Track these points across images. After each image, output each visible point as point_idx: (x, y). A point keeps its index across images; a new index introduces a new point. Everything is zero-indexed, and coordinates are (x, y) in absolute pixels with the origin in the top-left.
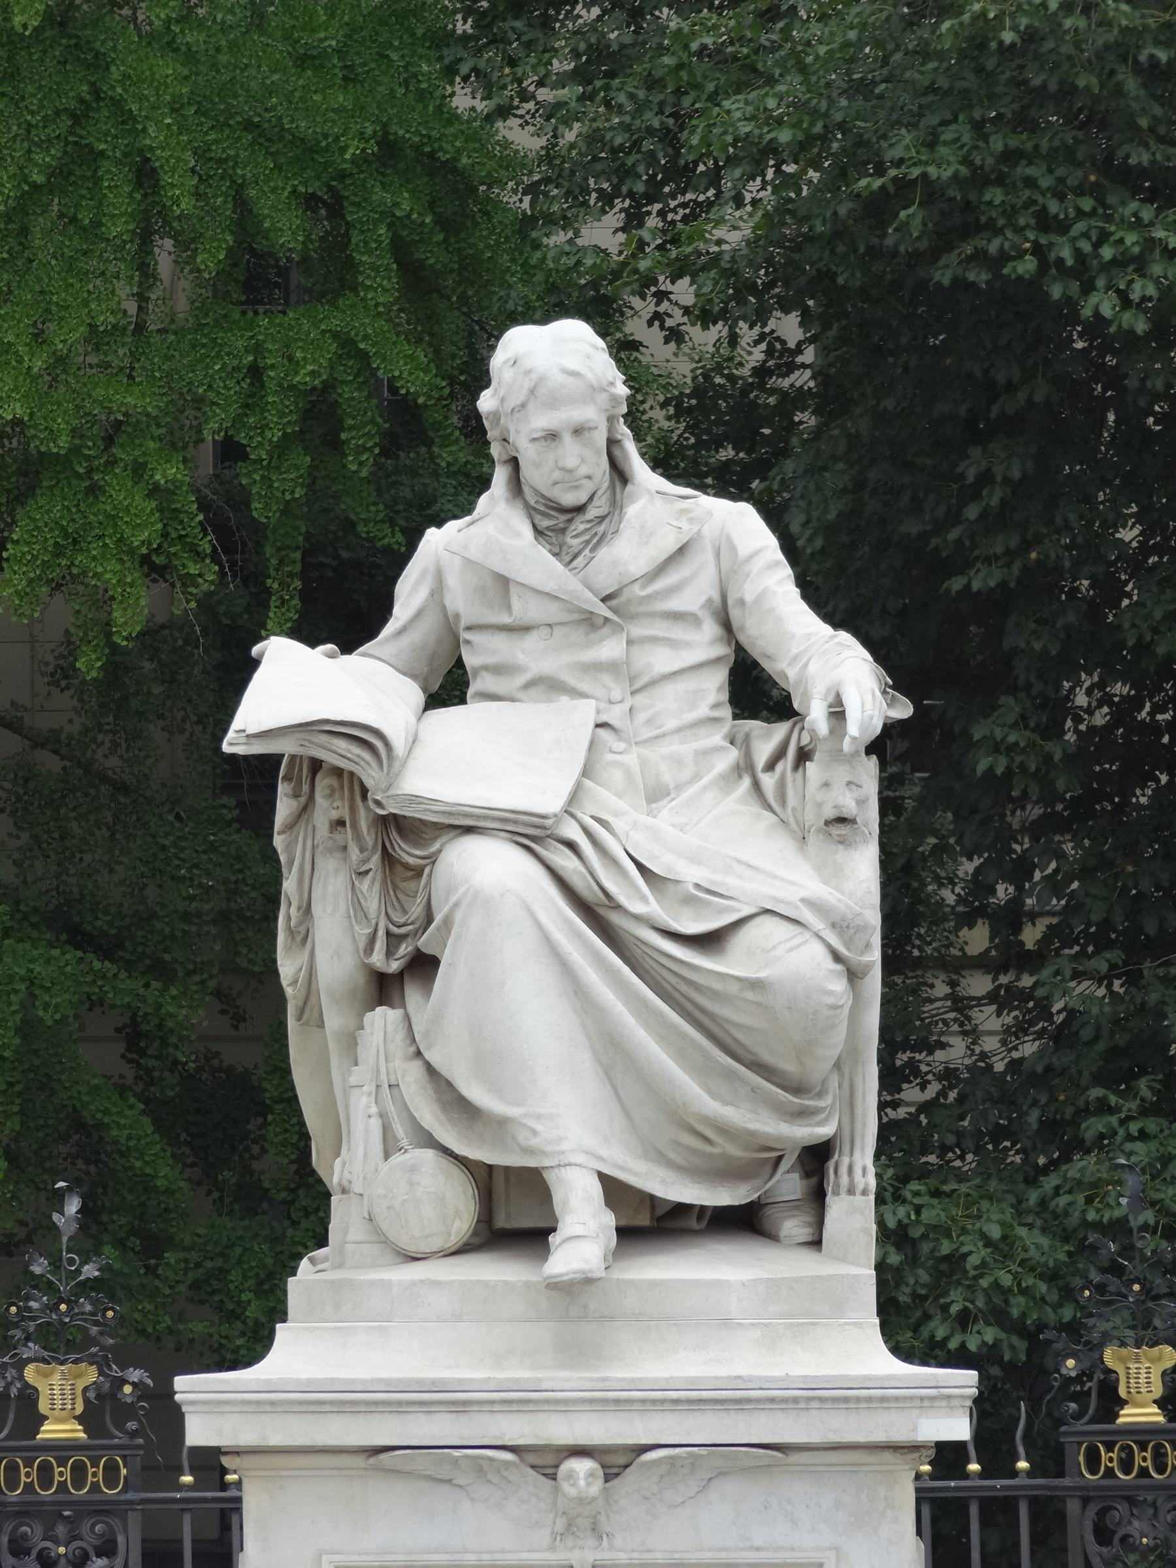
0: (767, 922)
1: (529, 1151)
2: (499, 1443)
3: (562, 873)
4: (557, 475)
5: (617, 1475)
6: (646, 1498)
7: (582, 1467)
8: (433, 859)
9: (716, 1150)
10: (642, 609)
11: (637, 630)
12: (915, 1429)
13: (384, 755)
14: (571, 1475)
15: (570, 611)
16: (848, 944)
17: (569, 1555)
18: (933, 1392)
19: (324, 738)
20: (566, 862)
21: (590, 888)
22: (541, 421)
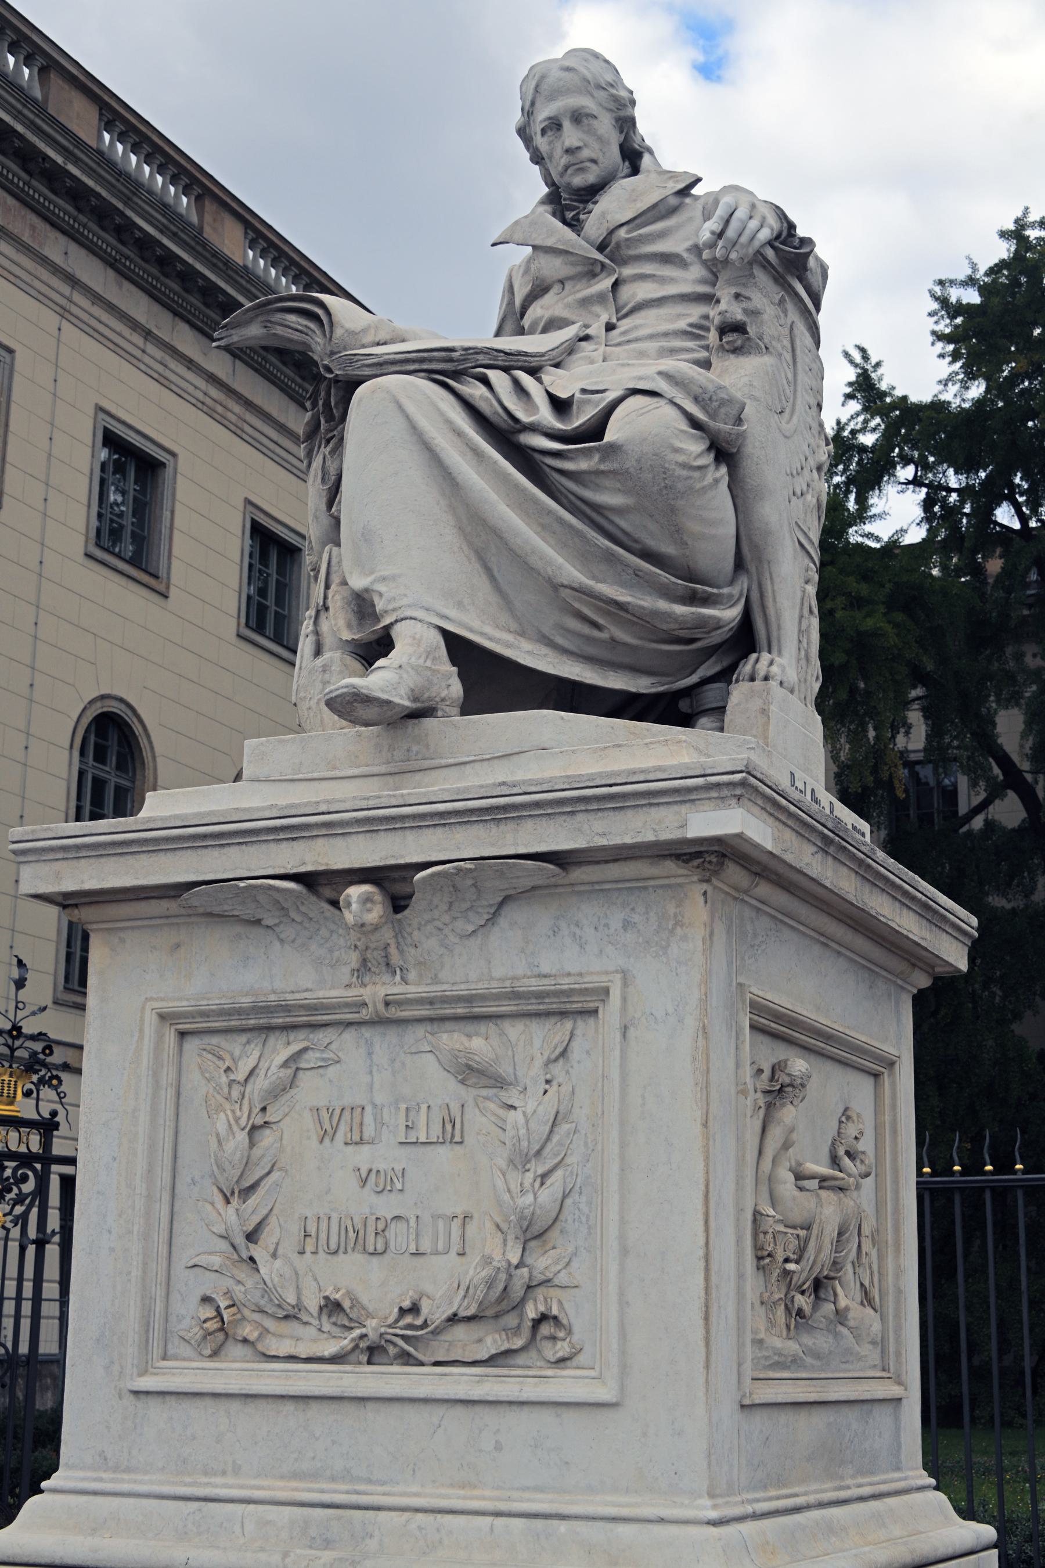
2: (282, 871)
3: (471, 400)
4: (565, 160)
5: (405, 907)
6: (440, 929)
7: (355, 892)
9: (604, 635)
10: (632, 252)
11: (627, 271)
12: (683, 826)
13: (326, 326)
15: (573, 264)
16: (713, 416)
17: (362, 991)
18: (700, 781)
19: (278, 317)
20: (475, 391)
21: (496, 413)
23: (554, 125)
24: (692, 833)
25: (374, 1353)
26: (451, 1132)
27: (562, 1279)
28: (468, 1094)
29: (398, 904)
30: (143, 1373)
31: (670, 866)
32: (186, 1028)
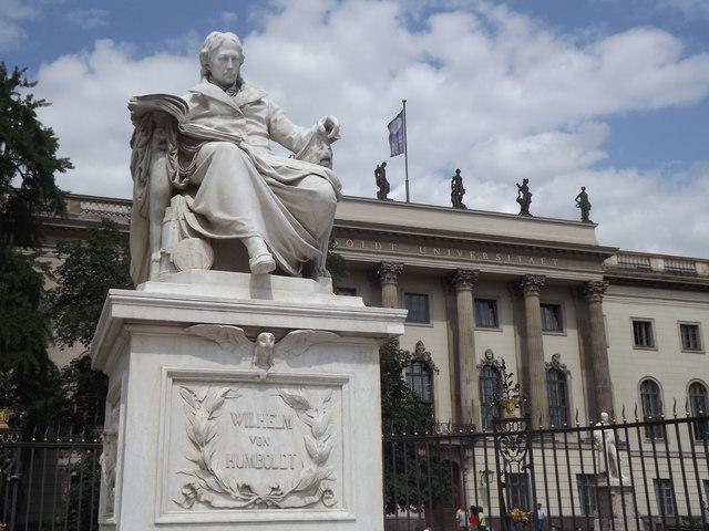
0: (312, 176)
1: (241, 232)
7: (269, 335)
8: (198, 150)
14: (264, 339)
19: (164, 102)
22: (222, 52)
23: (225, 58)
24: (388, 332)
25: (263, 504)
26: (288, 424)
27: (330, 477)
28: (293, 411)
29: (278, 340)
30: (162, 513)
31: (373, 341)
32: (178, 378)
